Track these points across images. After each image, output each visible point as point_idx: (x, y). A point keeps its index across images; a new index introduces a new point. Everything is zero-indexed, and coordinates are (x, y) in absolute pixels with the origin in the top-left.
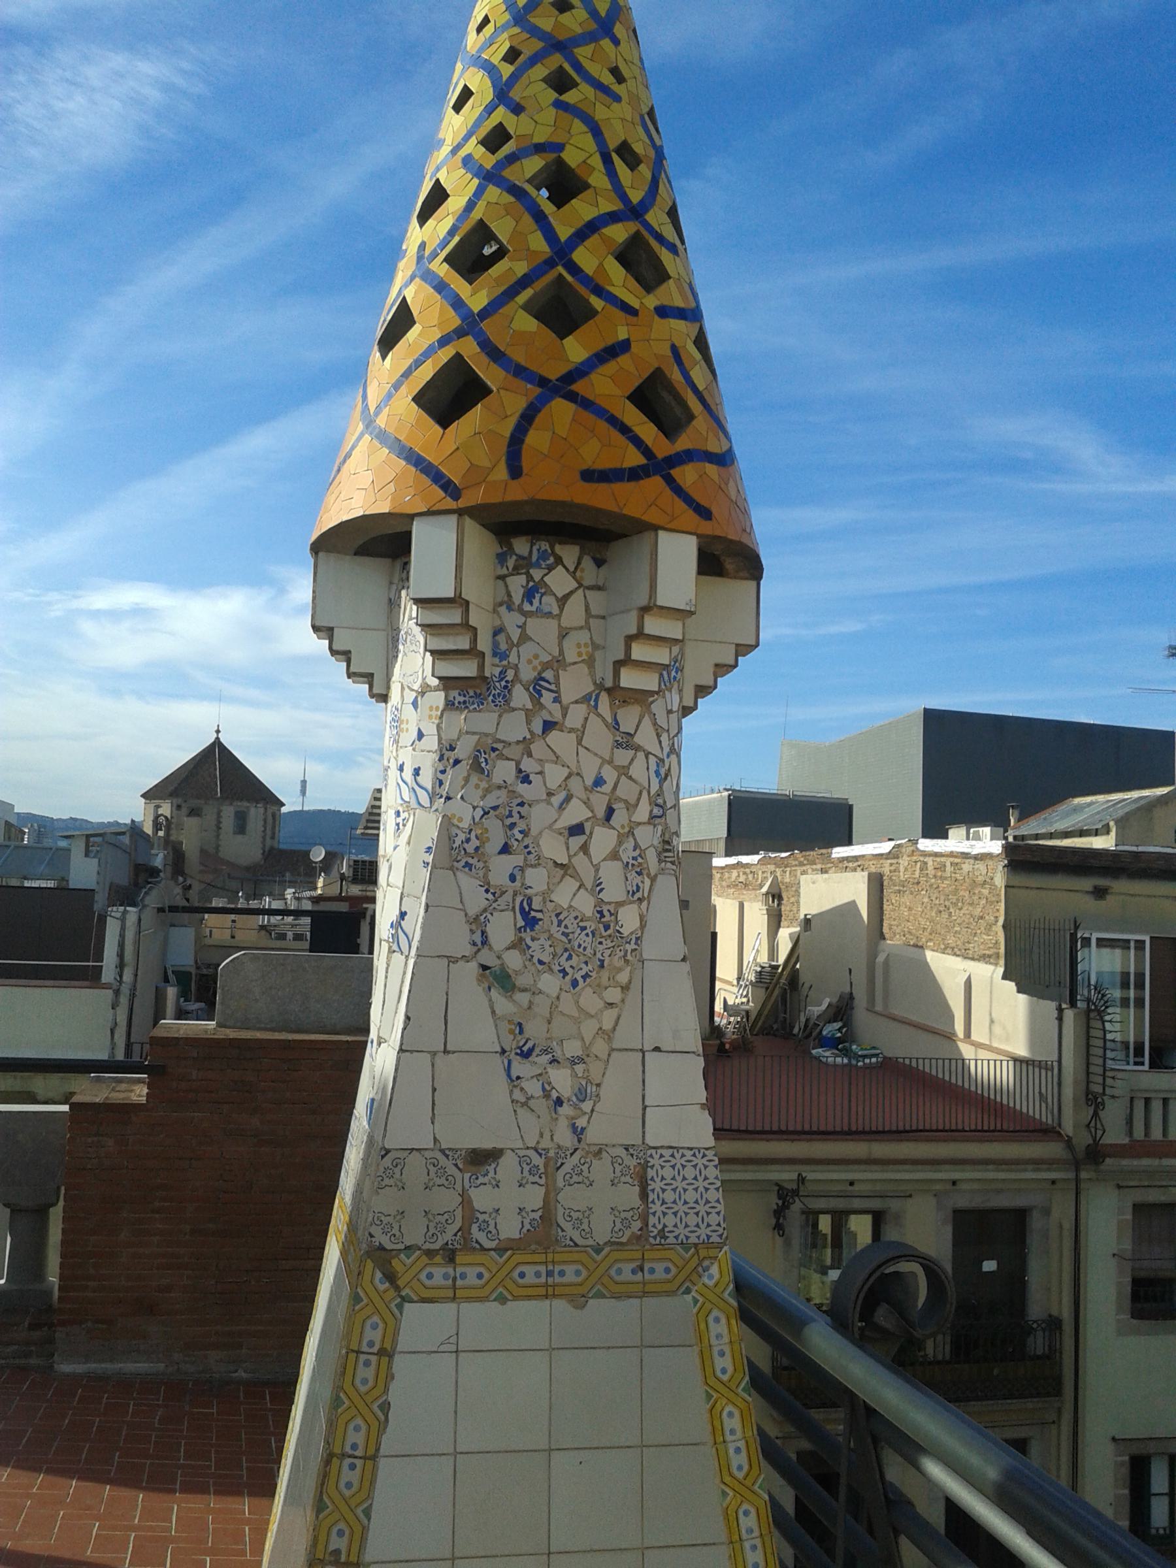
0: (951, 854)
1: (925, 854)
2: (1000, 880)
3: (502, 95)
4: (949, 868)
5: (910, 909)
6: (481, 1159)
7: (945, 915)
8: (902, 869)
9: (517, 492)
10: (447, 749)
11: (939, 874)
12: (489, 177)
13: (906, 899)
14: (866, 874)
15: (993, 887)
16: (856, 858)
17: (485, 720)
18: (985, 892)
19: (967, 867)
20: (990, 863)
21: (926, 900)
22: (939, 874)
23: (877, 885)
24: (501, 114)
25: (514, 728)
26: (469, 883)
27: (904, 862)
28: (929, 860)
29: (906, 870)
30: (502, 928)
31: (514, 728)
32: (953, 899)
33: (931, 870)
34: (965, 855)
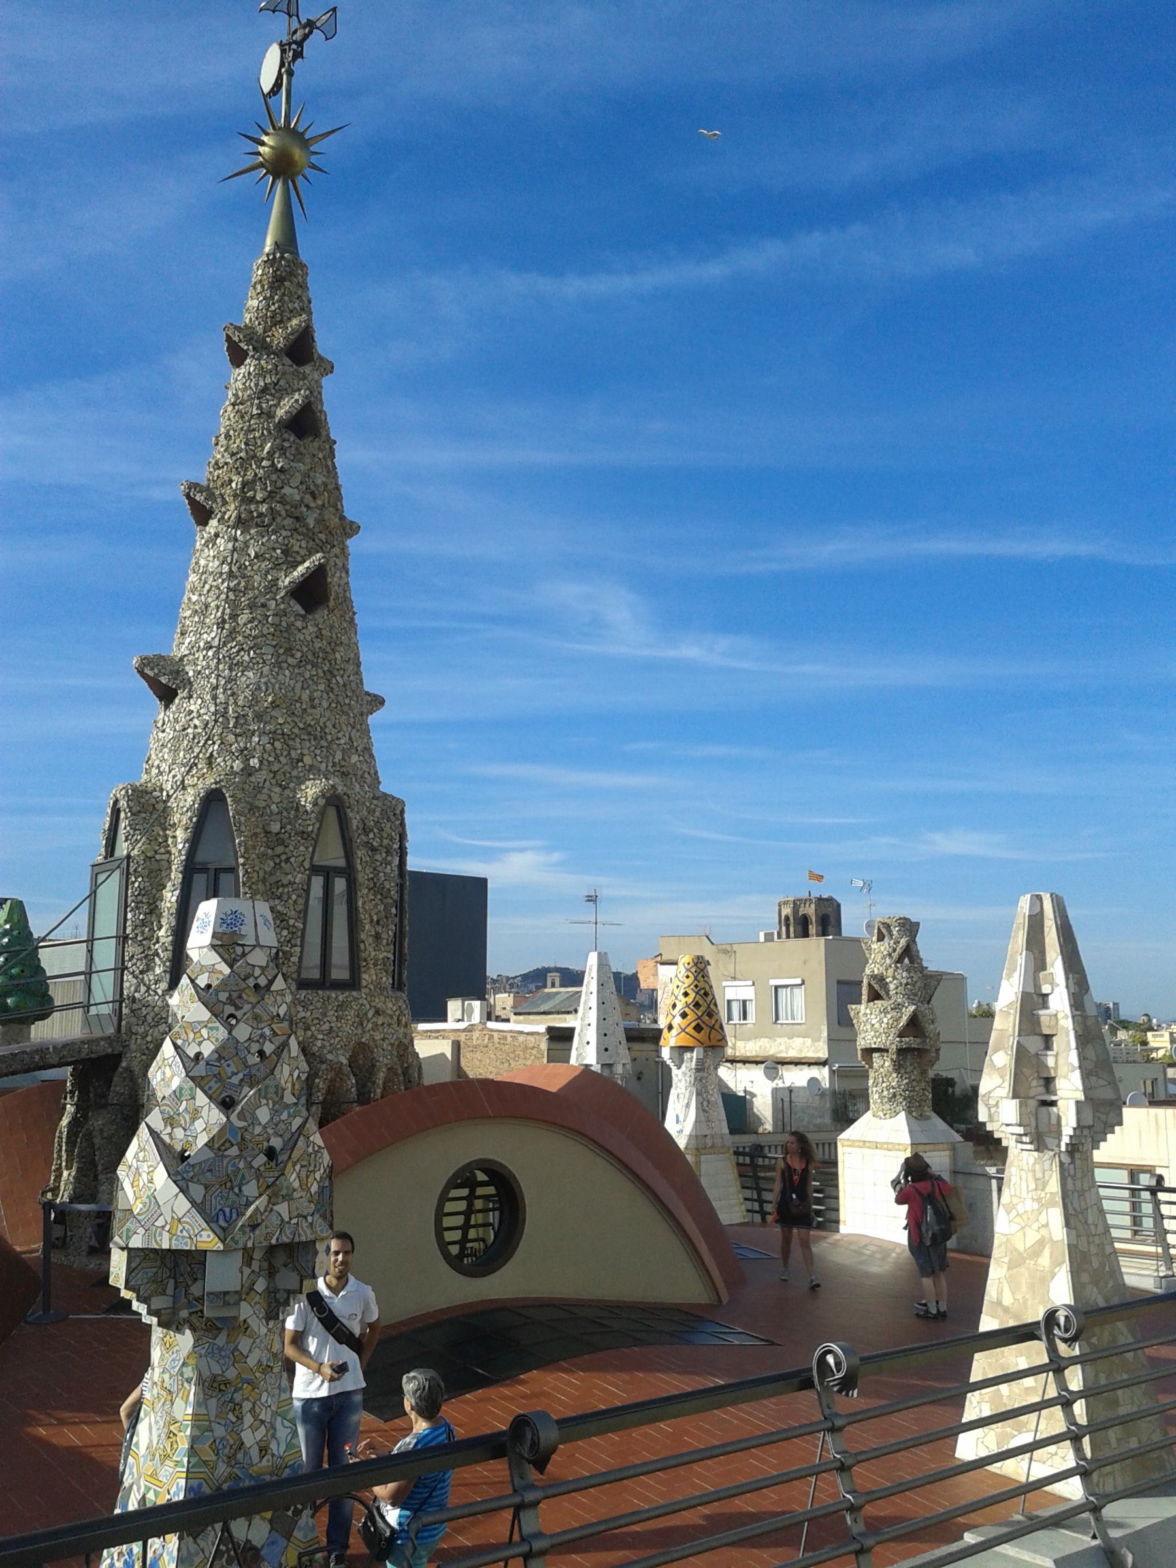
0: (511, 1031)
1: (492, 1030)
2: (544, 1046)
3: (696, 979)
4: (509, 1039)
5: (480, 1061)
6: (706, 1136)
7: (506, 1065)
8: (474, 1038)
9: (711, 1044)
10: (696, 1078)
11: (502, 1041)
12: (697, 993)
13: (478, 1055)
14: (450, 1041)
15: (539, 1050)
16: (438, 1031)
17: (701, 1074)
18: (534, 1052)
19: (521, 1038)
20: (537, 1037)
21: (493, 1056)
22: (502, 1041)
23: (457, 1046)
24: (696, 982)
25: (705, 1075)
26: (700, 1098)
27: (476, 1034)
28: (495, 1034)
29: (478, 1039)
30: (705, 1103)
31: (705, 1075)
32: (513, 1056)
33: (496, 1040)
34: (521, 1033)
